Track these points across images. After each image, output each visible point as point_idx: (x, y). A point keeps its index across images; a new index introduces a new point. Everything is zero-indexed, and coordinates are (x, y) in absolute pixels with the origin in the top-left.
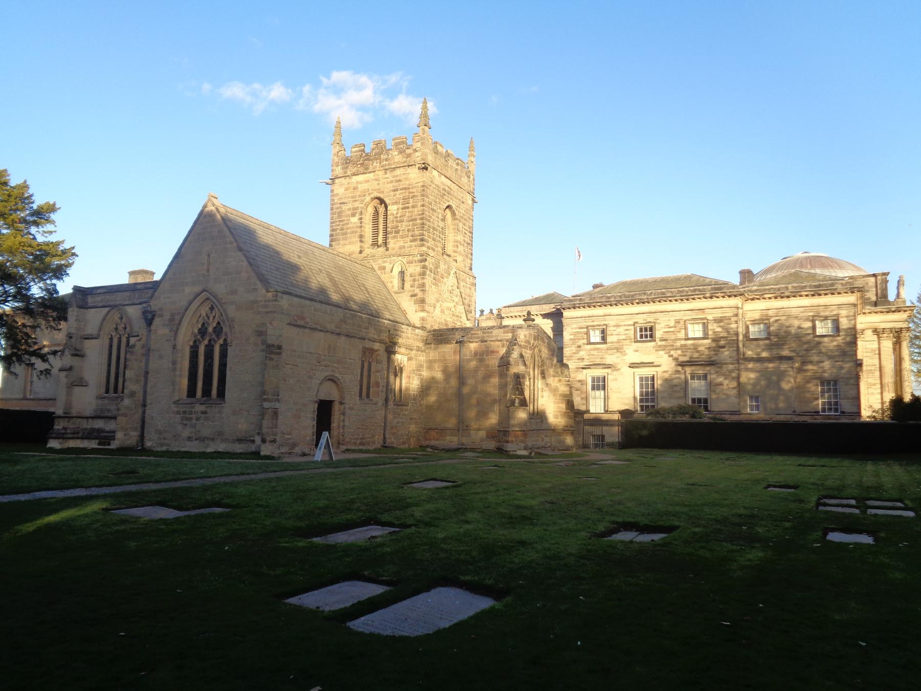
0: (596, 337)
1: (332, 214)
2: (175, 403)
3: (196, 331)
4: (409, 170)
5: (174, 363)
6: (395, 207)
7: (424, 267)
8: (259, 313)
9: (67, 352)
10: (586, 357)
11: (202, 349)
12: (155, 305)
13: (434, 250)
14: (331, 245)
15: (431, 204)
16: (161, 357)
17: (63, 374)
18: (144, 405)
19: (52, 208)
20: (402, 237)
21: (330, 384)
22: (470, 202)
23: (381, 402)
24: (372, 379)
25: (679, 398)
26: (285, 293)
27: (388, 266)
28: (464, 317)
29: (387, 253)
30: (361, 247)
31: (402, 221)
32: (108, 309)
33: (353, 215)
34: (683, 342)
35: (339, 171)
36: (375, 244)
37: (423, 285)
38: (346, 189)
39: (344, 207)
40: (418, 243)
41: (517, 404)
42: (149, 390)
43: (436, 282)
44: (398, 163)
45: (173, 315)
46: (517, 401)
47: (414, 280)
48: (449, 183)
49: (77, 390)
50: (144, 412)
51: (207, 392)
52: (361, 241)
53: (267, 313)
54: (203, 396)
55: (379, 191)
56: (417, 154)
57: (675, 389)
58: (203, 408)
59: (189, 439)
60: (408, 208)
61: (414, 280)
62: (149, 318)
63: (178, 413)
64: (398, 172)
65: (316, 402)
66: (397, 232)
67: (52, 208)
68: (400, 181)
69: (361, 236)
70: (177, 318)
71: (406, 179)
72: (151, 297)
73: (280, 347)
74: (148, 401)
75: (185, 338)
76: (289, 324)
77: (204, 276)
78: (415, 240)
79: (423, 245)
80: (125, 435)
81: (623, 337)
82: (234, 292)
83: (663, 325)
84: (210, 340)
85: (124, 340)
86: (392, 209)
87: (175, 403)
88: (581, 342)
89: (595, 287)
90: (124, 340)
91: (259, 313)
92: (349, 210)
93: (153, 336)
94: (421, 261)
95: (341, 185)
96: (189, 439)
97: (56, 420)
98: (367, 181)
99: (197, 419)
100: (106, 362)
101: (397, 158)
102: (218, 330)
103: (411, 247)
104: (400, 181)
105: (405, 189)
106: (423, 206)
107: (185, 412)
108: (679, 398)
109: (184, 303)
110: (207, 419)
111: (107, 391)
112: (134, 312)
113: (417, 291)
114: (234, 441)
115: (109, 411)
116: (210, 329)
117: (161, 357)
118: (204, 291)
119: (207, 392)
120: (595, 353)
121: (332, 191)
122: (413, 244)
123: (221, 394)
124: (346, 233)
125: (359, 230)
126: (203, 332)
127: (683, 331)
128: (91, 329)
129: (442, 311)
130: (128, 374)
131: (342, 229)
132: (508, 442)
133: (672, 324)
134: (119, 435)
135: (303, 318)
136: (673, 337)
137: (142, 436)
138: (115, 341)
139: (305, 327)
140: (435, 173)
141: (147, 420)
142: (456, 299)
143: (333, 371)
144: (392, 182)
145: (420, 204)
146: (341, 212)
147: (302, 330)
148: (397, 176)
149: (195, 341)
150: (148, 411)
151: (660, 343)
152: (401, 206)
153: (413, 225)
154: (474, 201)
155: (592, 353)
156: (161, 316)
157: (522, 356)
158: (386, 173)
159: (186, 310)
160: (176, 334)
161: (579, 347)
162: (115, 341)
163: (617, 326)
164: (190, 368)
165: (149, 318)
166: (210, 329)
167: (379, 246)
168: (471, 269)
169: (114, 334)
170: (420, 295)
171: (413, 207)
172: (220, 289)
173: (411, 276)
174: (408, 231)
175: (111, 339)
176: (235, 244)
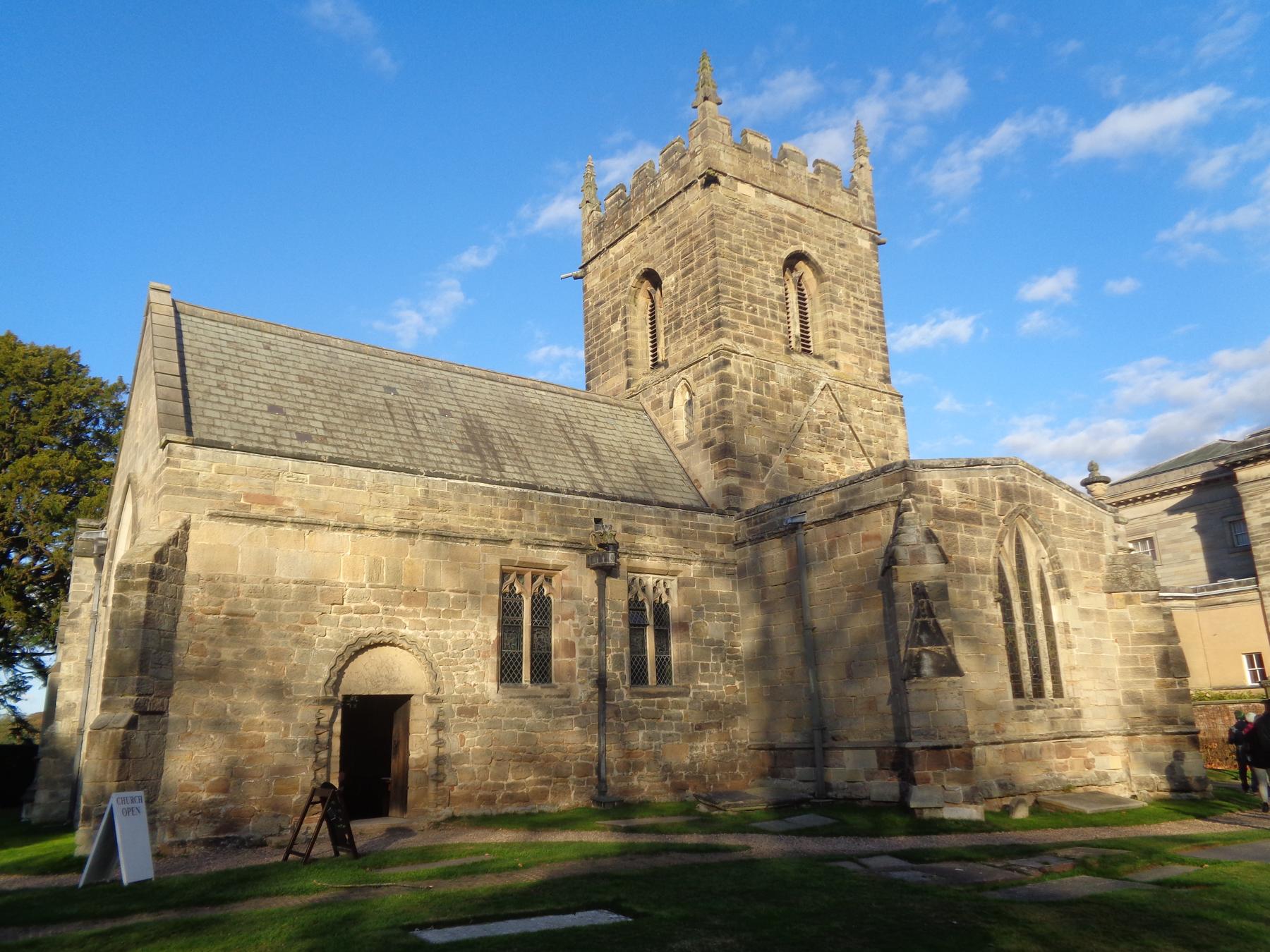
1: (587, 329)
4: (688, 196)
6: (672, 278)
7: (724, 379)
14: (588, 387)
15: (739, 250)
22: (866, 244)
30: (629, 375)
31: (684, 301)
33: (614, 319)
39: (603, 309)
40: (713, 332)
41: (927, 670)
46: (927, 661)
48: (793, 207)
55: (648, 258)
60: (692, 269)
61: (708, 412)
65: (326, 702)
68: (676, 223)
76: (212, 516)
78: (707, 329)
79: (720, 335)
80: (53, 795)
94: (716, 368)
95: (596, 270)
103: (702, 345)
104: (676, 223)
105: (684, 235)
106: (714, 255)
122: (704, 338)
124: (607, 357)
131: (601, 352)
135: (270, 500)
143: (389, 623)
144: (664, 231)
145: (709, 253)
147: (264, 529)
148: (671, 217)
152: (680, 271)
153: (703, 300)
158: (654, 220)
168: (887, 380)
171: (699, 265)
174: (695, 315)
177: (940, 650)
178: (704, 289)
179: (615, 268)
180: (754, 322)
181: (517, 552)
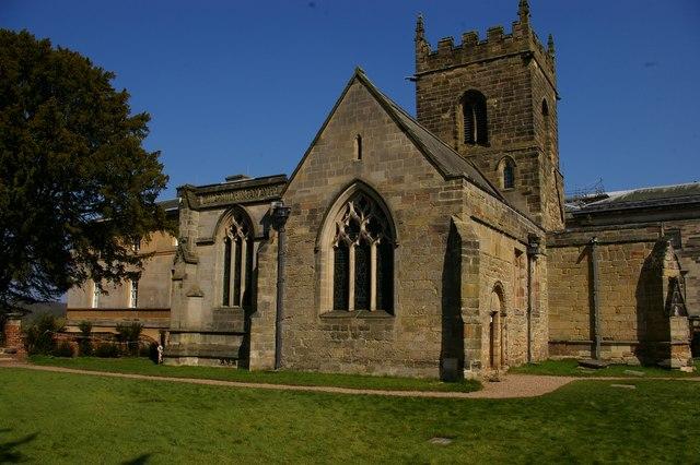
3: (342, 230)
8: (438, 204)
11: (352, 251)
16: (300, 262)
19: (145, 118)
20: (506, 131)
27: (492, 164)
31: (504, 115)
33: (445, 111)
35: (425, 66)
36: (469, 141)
37: (538, 181)
41: (676, 313)
42: (284, 300)
45: (313, 211)
47: (526, 177)
51: (363, 303)
52: (456, 138)
54: (356, 307)
55: (474, 84)
56: (521, 43)
58: (361, 322)
61: (526, 177)
67: (145, 118)
72: (284, 192)
73: (477, 245)
75: (328, 238)
78: (523, 134)
80: (260, 354)
82: (400, 180)
83: (688, 232)
86: (492, 102)
92: (439, 106)
95: (428, 80)
98: (458, 75)
99: (355, 336)
101: (495, 49)
104: (500, 72)
107: (336, 328)
109: (327, 197)
110: (368, 337)
111: (226, 302)
113: (530, 188)
114: (409, 364)
115: (232, 326)
116: (363, 228)
119: (363, 303)
123: (387, 303)
125: (452, 127)
126: (353, 227)
138: (234, 245)
151: (686, 249)
162: (234, 245)
164: (336, 274)
167: (473, 143)
170: (534, 193)
171: (518, 98)
172: (377, 178)
173: (522, 172)
175: (228, 243)
177: (681, 305)
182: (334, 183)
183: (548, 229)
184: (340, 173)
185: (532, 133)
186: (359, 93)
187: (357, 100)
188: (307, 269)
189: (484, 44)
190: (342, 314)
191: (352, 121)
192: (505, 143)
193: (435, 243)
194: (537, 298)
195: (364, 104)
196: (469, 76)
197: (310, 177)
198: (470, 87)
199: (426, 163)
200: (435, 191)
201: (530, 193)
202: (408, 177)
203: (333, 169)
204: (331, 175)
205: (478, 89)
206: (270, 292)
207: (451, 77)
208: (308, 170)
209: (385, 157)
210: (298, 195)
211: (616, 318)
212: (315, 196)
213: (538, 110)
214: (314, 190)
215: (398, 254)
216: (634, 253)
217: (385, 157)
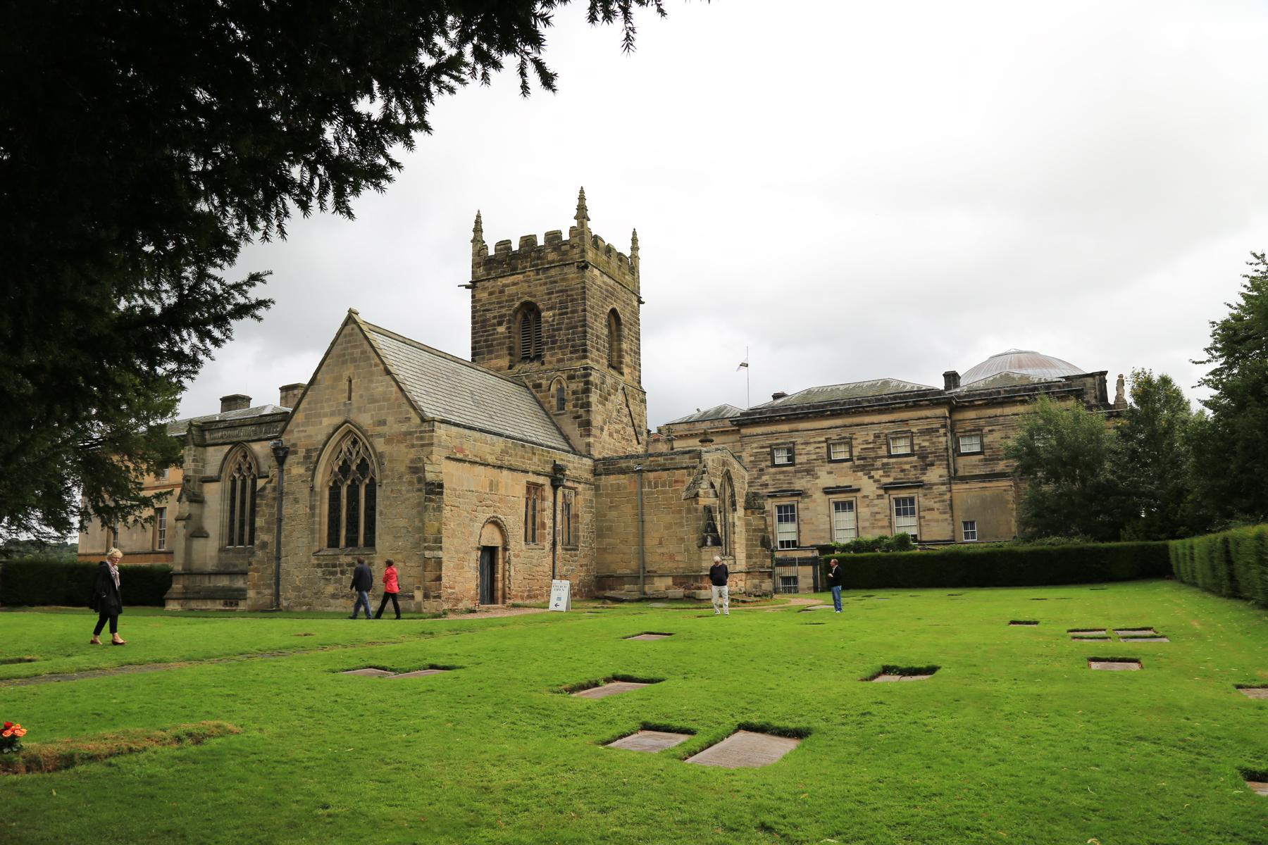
0: (781, 458)
2: (314, 554)
4: (566, 270)
5: (312, 508)
7: (587, 383)
9: (184, 499)
10: (770, 482)
11: (344, 491)
12: (286, 440)
13: (597, 362)
14: (473, 360)
16: (296, 501)
17: (181, 524)
18: (278, 559)
20: (560, 348)
21: (490, 527)
22: (636, 304)
23: (548, 545)
24: (538, 520)
25: (883, 527)
26: (443, 422)
28: (635, 442)
29: (543, 368)
31: (560, 329)
32: (229, 447)
33: (500, 324)
34: (885, 460)
35: (481, 271)
37: (588, 404)
38: (491, 294)
39: (489, 315)
42: (283, 539)
43: (604, 399)
44: (553, 262)
45: (308, 451)
46: (709, 539)
47: (577, 399)
48: (612, 282)
49: (198, 544)
50: (278, 566)
51: (352, 542)
52: (510, 354)
53: (423, 446)
54: (347, 545)
55: (530, 294)
56: (575, 251)
57: (878, 517)
59: (334, 596)
61: (577, 399)
62: (281, 455)
63: (319, 566)
64: (553, 272)
66: (554, 342)
68: (556, 282)
69: (510, 348)
70: (315, 454)
71: (563, 280)
72: (283, 431)
73: (441, 486)
74: (283, 554)
75: (322, 478)
76: (448, 458)
77: (345, 404)
79: (585, 357)
80: (258, 593)
81: (814, 457)
82: (382, 423)
83: (860, 441)
84: (353, 481)
85: (249, 482)
87: (314, 554)
88: (763, 465)
89: (776, 397)
90: (249, 482)
91: (413, 446)
92: (495, 317)
93: (285, 478)
95: (484, 289)
96: (334, 596)
97: (174, 579)
98: (514, 284)
99: (343, 573)
100: (228, 508)
101: (552, 256)
102: (363, 467)
104: (556, 282)
105: (562, 291)
107: (326, 565)
108: (883, 527)
109: (322, 437)
111: (231, 543)
112: (261, 449)
115: (235, 566)
117: (296, 501)
118: (346, 422)
119: (352, 542)
120: (781, 477)
121: (473, 297)
123: (370, 542)
126: (345, 469)
127: (884, 447)
128: (211, 470)
129: (611, 435)
130: (259, 522)
131: (486, 341)
132: (699, 588)
133: (871, 438)
134: (251, 594)
135: (462, 451)
136: (872, 454)
137: (277, 595)
138: (239, 483)
139: (465, 461)
140: (596, 272)
141: (283, 576)
142: (625, 420)
144: (545, 284)
146: (484, 321)
147: (461, 464)
149: (335, 482)
150: (283, 565)
151: (857, 463)
154: (640, 302)
155: (778, 477)
156: (295, 453)
157: (712, 486)
159: (325, 445)
160: (314, 474)
161: (762, 470)
162: (239, 483)
163: (806, 443)
165: (281, 455)
166: (354, 467)
169: (237, 475)
171: (573, 312)
172: (365, 420)
174: (568, 340)
175: (234, 481)
176: (382, 367)
178: (576, 327)
179: (502, 292)
180: (598, 350)
181: (533, 478)
182: (328, 423)
183: (597, 456)
184: (332, 414)
185: (585, 351)
186: (351, 335)
187: (349, 342)
188: (302, 509)
189: (540, 250)
190: (331, 551)
191: (344, 362)
192: (560, 361)
193: (411, 483)
194: (577, 529)
195: (355, 347)
196: (525, 285)
197: (307, 417)
198: (527, 298)
199: (406, 407)
200: (411, 433)
201: (579, 417)
202: (390, 419)
203: (327, 410)
204: (325, 415)
205: (533, 300)
206: (269, 530)
207: (508, 286)
208: (305, 410)
209: (373, 400)
210: (296, 435)
211: (660, 550)
212: (310, 436)
213: (599, 327)
214: (311, 430)
215: (379, 492)
216: (676, 481)
217: (373, 400)
